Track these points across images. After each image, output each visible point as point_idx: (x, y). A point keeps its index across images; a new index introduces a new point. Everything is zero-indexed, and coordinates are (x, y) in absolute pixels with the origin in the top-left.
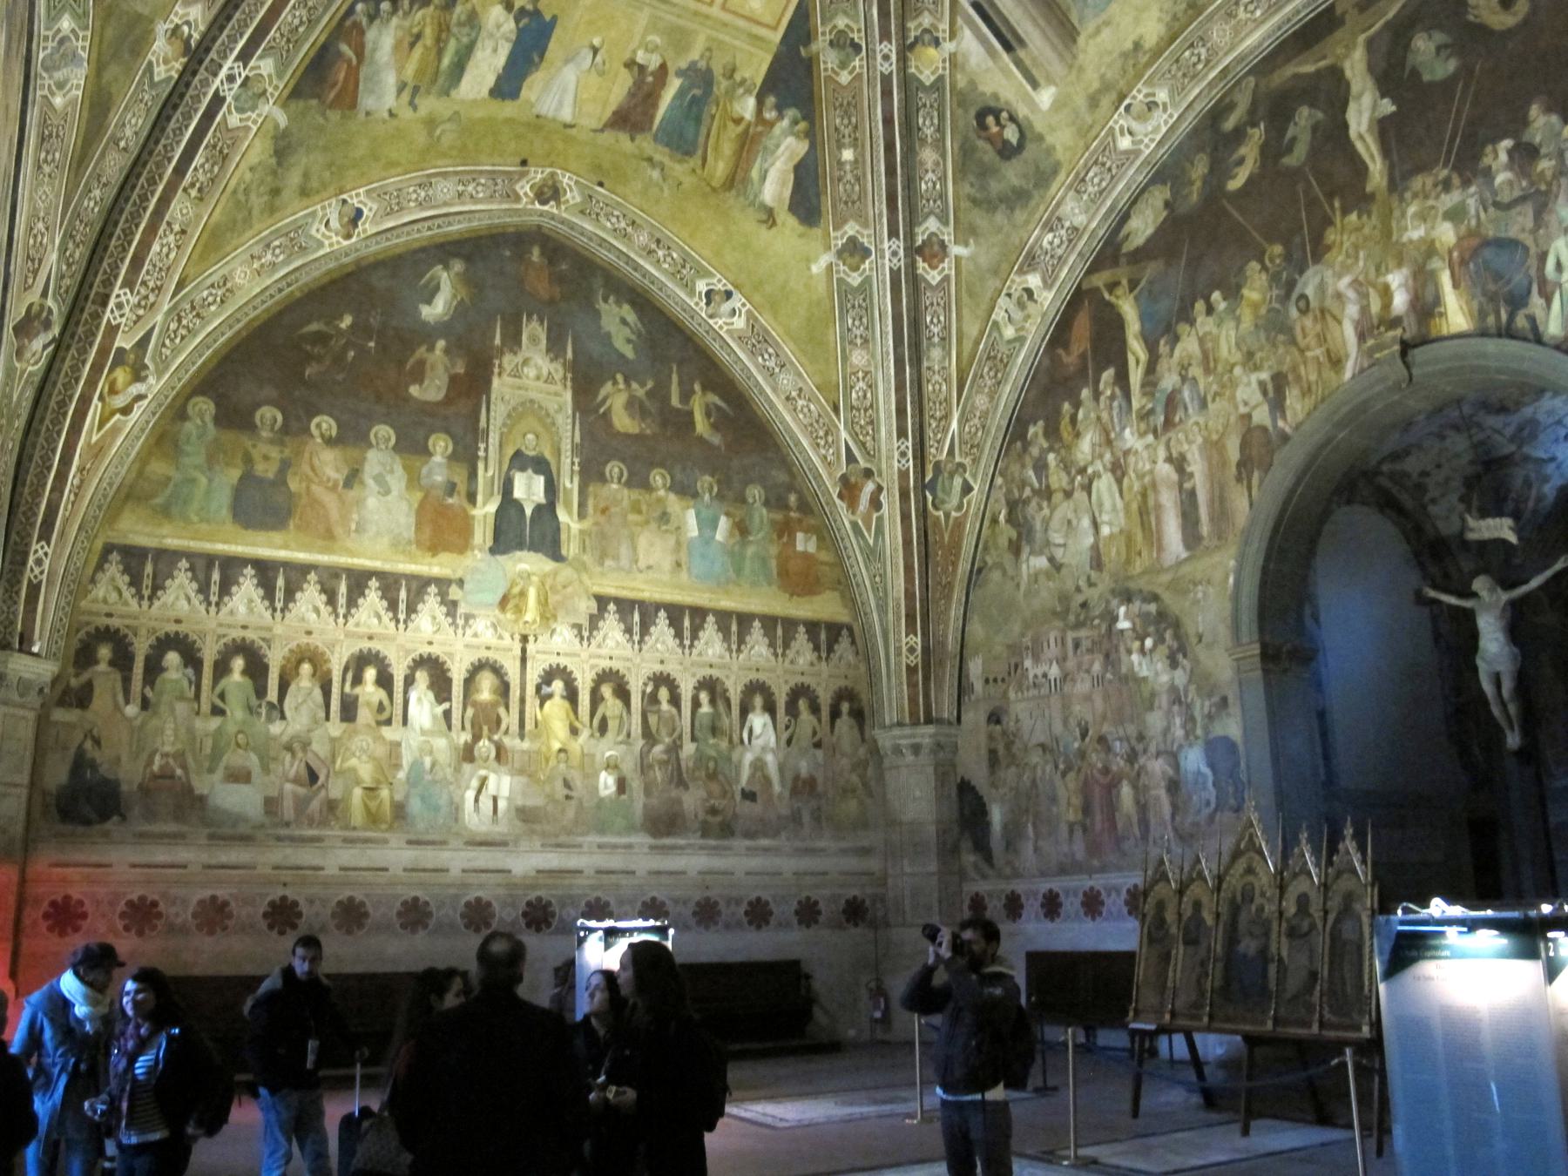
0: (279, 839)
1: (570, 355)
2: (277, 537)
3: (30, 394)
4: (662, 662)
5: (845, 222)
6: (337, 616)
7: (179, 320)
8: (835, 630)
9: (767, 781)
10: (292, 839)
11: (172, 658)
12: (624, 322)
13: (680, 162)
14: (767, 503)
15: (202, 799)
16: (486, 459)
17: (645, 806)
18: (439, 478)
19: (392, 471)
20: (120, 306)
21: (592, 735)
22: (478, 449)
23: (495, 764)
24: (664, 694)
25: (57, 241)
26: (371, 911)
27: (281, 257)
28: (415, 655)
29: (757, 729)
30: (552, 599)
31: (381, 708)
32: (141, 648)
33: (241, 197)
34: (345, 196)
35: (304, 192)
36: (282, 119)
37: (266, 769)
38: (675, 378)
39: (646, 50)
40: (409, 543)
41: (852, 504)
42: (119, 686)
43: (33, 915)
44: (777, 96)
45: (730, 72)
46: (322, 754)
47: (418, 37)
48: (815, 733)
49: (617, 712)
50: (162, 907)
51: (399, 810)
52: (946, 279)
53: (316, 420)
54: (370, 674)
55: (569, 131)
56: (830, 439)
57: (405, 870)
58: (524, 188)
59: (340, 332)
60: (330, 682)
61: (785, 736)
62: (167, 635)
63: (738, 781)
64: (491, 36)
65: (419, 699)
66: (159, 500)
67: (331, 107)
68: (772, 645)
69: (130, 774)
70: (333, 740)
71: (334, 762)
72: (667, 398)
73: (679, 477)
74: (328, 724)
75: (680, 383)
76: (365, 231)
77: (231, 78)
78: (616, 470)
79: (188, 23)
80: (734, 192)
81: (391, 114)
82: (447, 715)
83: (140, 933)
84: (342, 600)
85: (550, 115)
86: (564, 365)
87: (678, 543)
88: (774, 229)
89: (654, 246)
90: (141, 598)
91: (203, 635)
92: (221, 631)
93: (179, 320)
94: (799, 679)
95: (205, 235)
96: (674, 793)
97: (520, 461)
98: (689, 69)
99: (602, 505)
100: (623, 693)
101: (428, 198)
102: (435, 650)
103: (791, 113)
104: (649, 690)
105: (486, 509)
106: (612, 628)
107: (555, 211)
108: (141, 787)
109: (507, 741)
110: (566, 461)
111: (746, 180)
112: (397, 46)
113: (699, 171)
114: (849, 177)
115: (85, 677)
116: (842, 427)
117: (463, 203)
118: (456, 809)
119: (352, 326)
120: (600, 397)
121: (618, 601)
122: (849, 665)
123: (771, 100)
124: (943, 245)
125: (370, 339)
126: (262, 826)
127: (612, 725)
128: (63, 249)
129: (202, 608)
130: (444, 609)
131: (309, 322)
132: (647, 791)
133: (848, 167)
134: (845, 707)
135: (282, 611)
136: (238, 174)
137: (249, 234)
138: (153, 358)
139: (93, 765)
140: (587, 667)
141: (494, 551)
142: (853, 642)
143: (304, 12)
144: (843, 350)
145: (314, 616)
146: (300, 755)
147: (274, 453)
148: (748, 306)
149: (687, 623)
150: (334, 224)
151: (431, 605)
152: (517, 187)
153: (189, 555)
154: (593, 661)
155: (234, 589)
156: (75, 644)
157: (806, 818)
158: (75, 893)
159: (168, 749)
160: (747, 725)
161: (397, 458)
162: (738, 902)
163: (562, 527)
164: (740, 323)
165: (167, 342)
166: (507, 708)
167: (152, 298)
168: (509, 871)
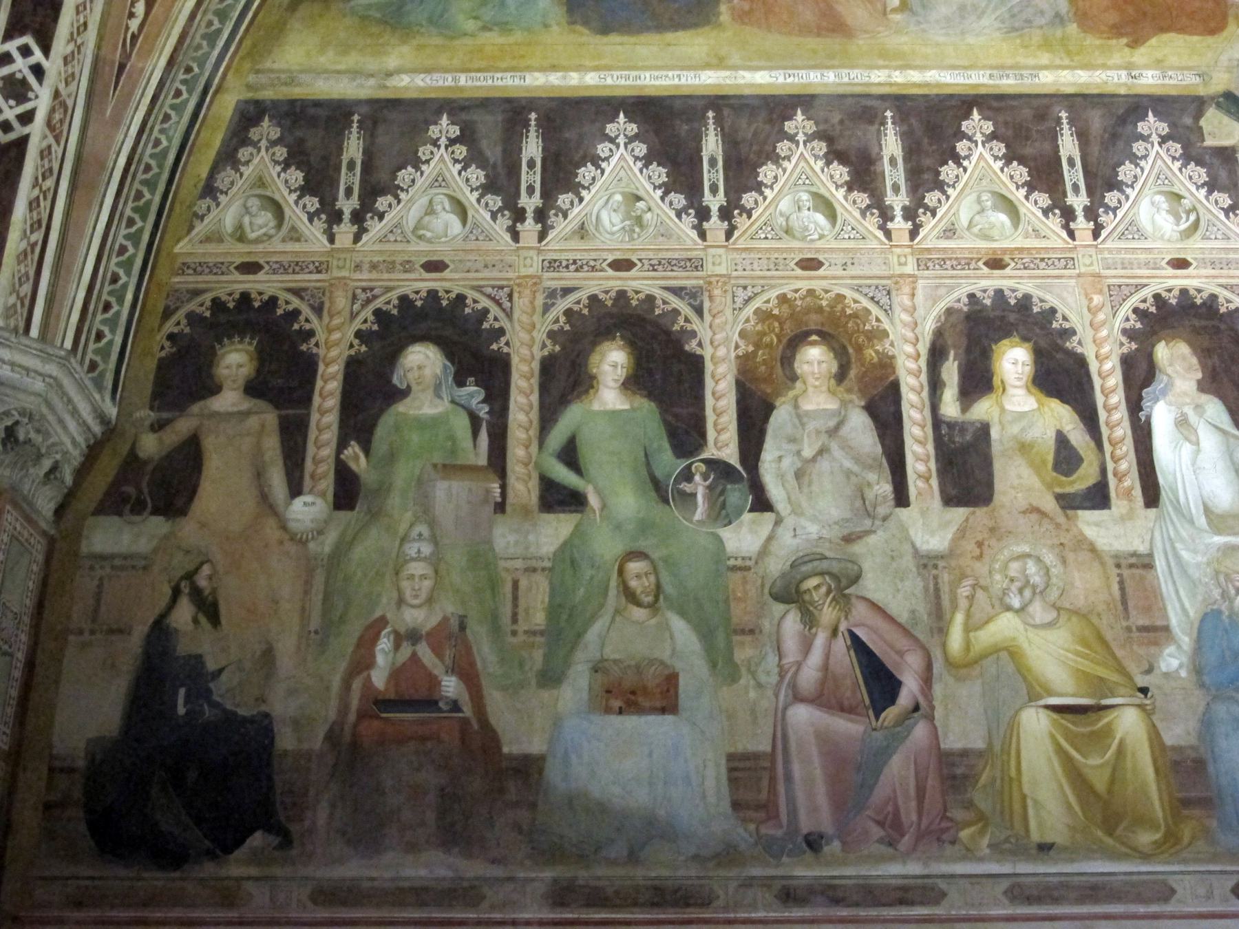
0: (789, 895)
2: (693, 43)
6: (886, 215)
31: (1066, 458)
40: (1059, 19)
42: (272, 445)
46: (899, 608)
62: (404, 299)
65: (1182, 423)
70: (927, 563)
71: (942, 630)
74: (903, 513)
84: (894, 174)
90: (336, 217)
91: (505, 296)
92: (553, 280)
108: (332, 737)
115: (183, 426)
126: (728, 855)
130: (1201, 174)
145: (820, 218)
146: (828, 614)
153: (454, 107)
155: (585, 173)
156: (158, 345)
159: (414, 617)
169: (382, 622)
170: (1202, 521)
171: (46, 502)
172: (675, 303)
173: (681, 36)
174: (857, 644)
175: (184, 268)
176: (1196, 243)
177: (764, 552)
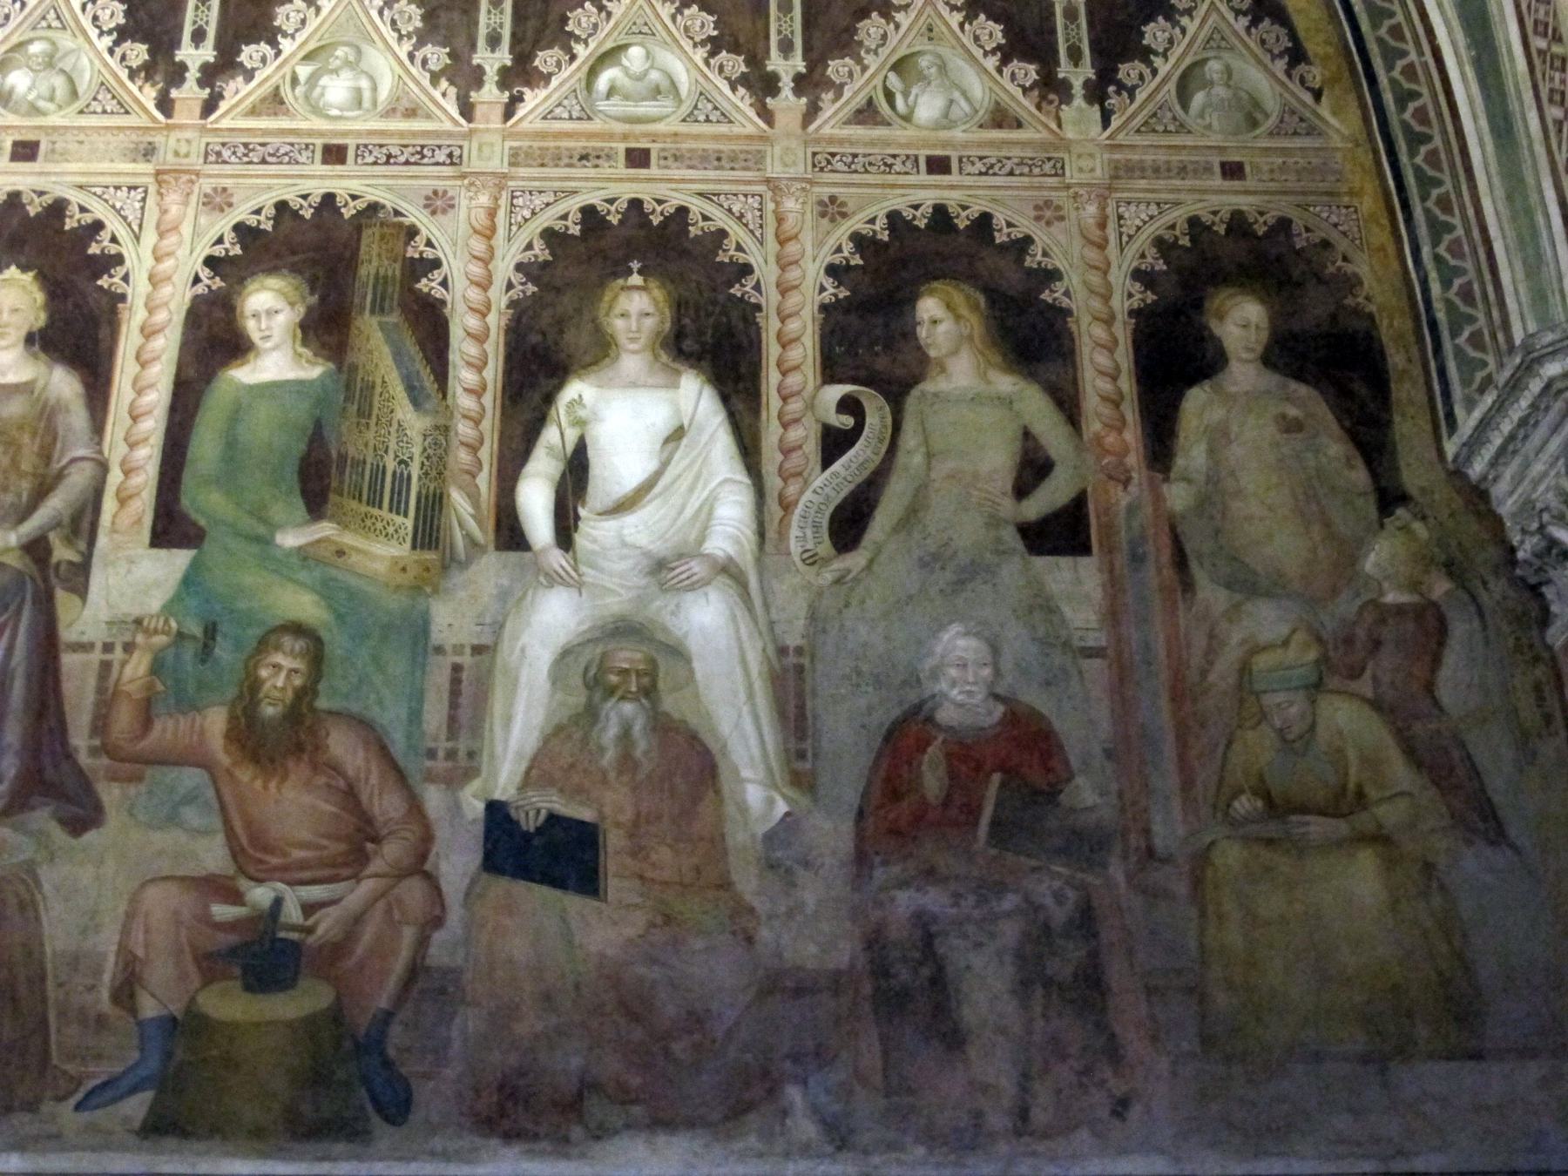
4: (25, 151)
63: (464, 768)
160: (554, 439)
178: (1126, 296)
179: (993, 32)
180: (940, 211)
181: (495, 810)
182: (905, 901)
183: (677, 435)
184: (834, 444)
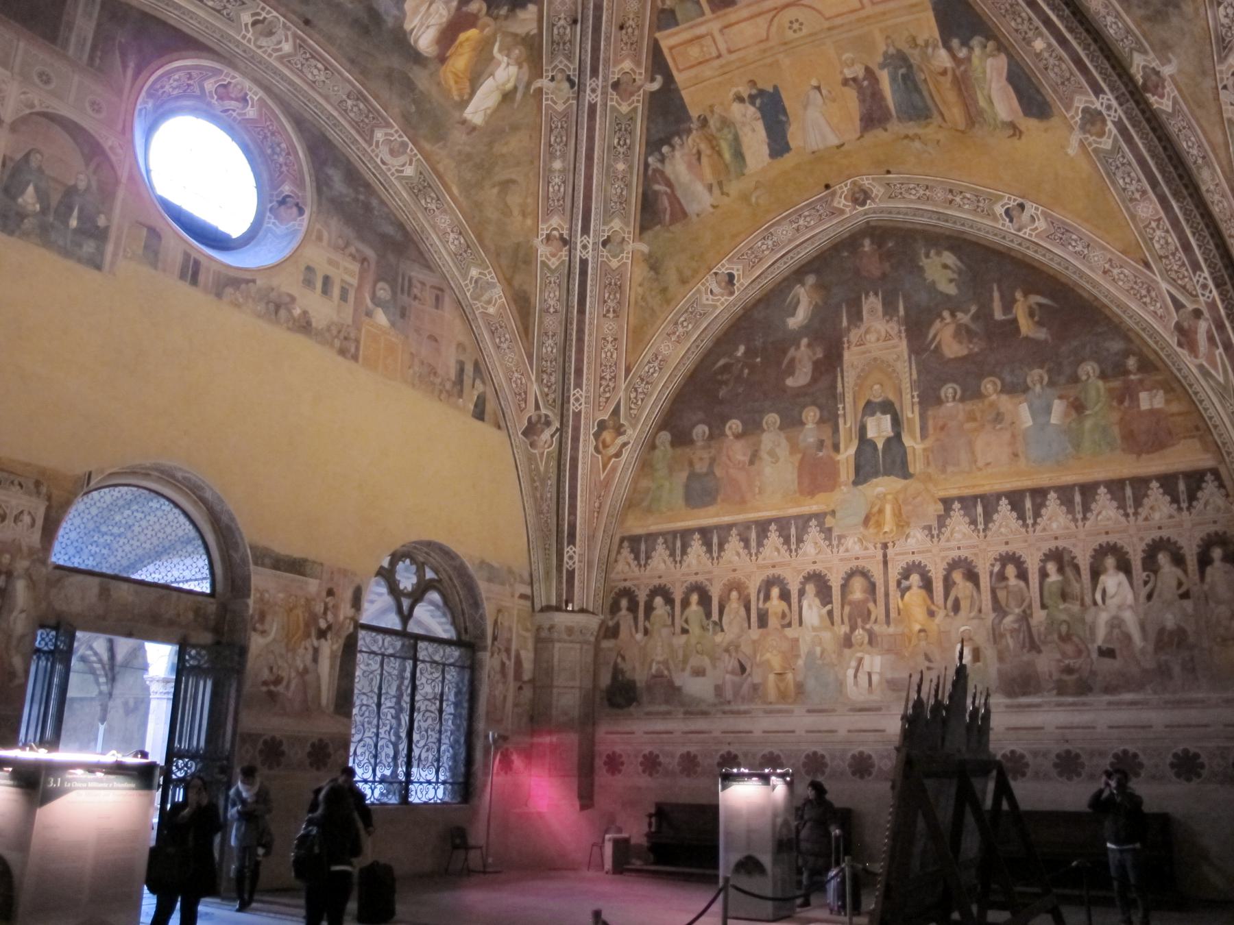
0: (724, 713)
1: (902, 312)
2: (712, 510)
3: (553, 464)
4: (1007, 543)
5: (1072, 100)
7: (636, 390)
8: (1195, 479)
9: (1128, 637)
10: (732, 712)
11: (659, 601)
12: (945, 266)
13: (927, 126)
14: (1103, 376)
15: (679, 689)
16: (844, 415)
17: (999, 671)
18: (811, 440)
19: (779, 445)
20: (577, 400)
21: (947, 615)
22: (838, 409)
23: (868, 648)
24: (1011, 571)
25: (533, 378)
26: (829, 762)
27: (690, 326)
28: (804, 573)
29: (1111, 589)
30: (905, 509)
31: (784, 616)
32: (642, 598)
33: (644, 304)
34: (714, 271)
35: (684, 281)
36: (644, 248)
37: (714, 667)
38: (996, 295)
39: (848, 66)
41: (1192, 347)
43: (599, 762)
44: (957, 36)
45: (913, 42)
47: (699, 153)
48: (1180, 584)
49: (968, 593)
50: (661, 759)
51: (800, 688)
52: (1175, 102)
53: (727, 426)
54: (775, 592)
55: (843, 149)
56: (1153, 294)
57: (808, 732)
58: (841, 202)
59: (738, 359)
60: (750, 601)
61: (1144, 592)
63: (1093, 641)
64: (744, 124)
65: (810, 606)
66: (645, 504)
67: (671, 225)
68: (1122, 506)
69: (640, 677)
70: (754, 642)
71: (755, 658)
72: (991, 315)
73: (1008, 378)
74: (751, 631)
75: (1002, 297)
76: (742, 285)
77: (585, 247)
78: (951, 390)
79: (555, 229)
80: (977, 126)
81: (714, 207)
82: (830, 613)
83: (651, 775)
84: (753, 544)
85: (821, 146)
86: (898, 321)
87: (1013, 436)
88: (1023, 137)
89: (950, 197)
93: (636, 390)
94: (1156, 534)
95: (630, 335)
96: (1026, 657)
97: (870, 408)
98: (885, 59)
99: (941, 423)
100: (972, 576)
101: (775, 244)
102: (818, 567)
103: (976, 42)
104: (996, 569)
105: (848, 453)
106: (958, 522)
107: (874, 206)
109: (876, 628)
110: (907, 398)
111: (980, 112)
112: (690, 166)
113: (944, 125)
114: (1052, 61)
115: (616, 619)
116: (1159, 279)
117: (803, 234)
118: (841, 684)
119: (745, 353)
120: (930, 336)
121: (961, 499)
122: (1218, 509)
123: (955, 43)
124: (1157, 73)
125: (757, 357)
126: (715, 705)
127: (964, 604)
128: (540, 380)
129: (672, 566)
130: (823, 535)
131: (718, 361)
132: (1001, 659)
133: (1046, 55)
134: (1217, 553)
135: (717, 559)
136: (633, 294)
137: (659, 322)
138: (626, 418)
139: (622, 672)
140: (938, 560)
141: (855, 483)
142: (1222, 485)
143: (620, 183)
144: (1128, 209)
145: (737, 558)
146: (734, 654)
147: (706, 455)
148: (1041, 208)
149: (1028, 504)
150: (716, 290)
151: (813, 532)
152: (835, 204)
154: (943, 554)
156: (610, 601)
157: (1177, 670)
158: (618, 749)
159: (660, 658)
161: (782, 435)
162: (1102, 754)
163: (909, 451)
164: (1041, 224)
165: (633, 406)
166: (875, 602)
167: (612, 385)
168: (883, 731)
169: (653, 660)
170: (810, 629)
171: (592, 639)
172: (707, 583)
173: (710, 508)
174: (739, 661)
175: (614, 581)
176: (820, 557)
177: (722, 642)
178: (1195, 550)
179: (1168, 498)
180: (1161, 538)
181: (1100, 649)
182: (1163, 658)
183: (1119, 584)
184: (1146, 583)
